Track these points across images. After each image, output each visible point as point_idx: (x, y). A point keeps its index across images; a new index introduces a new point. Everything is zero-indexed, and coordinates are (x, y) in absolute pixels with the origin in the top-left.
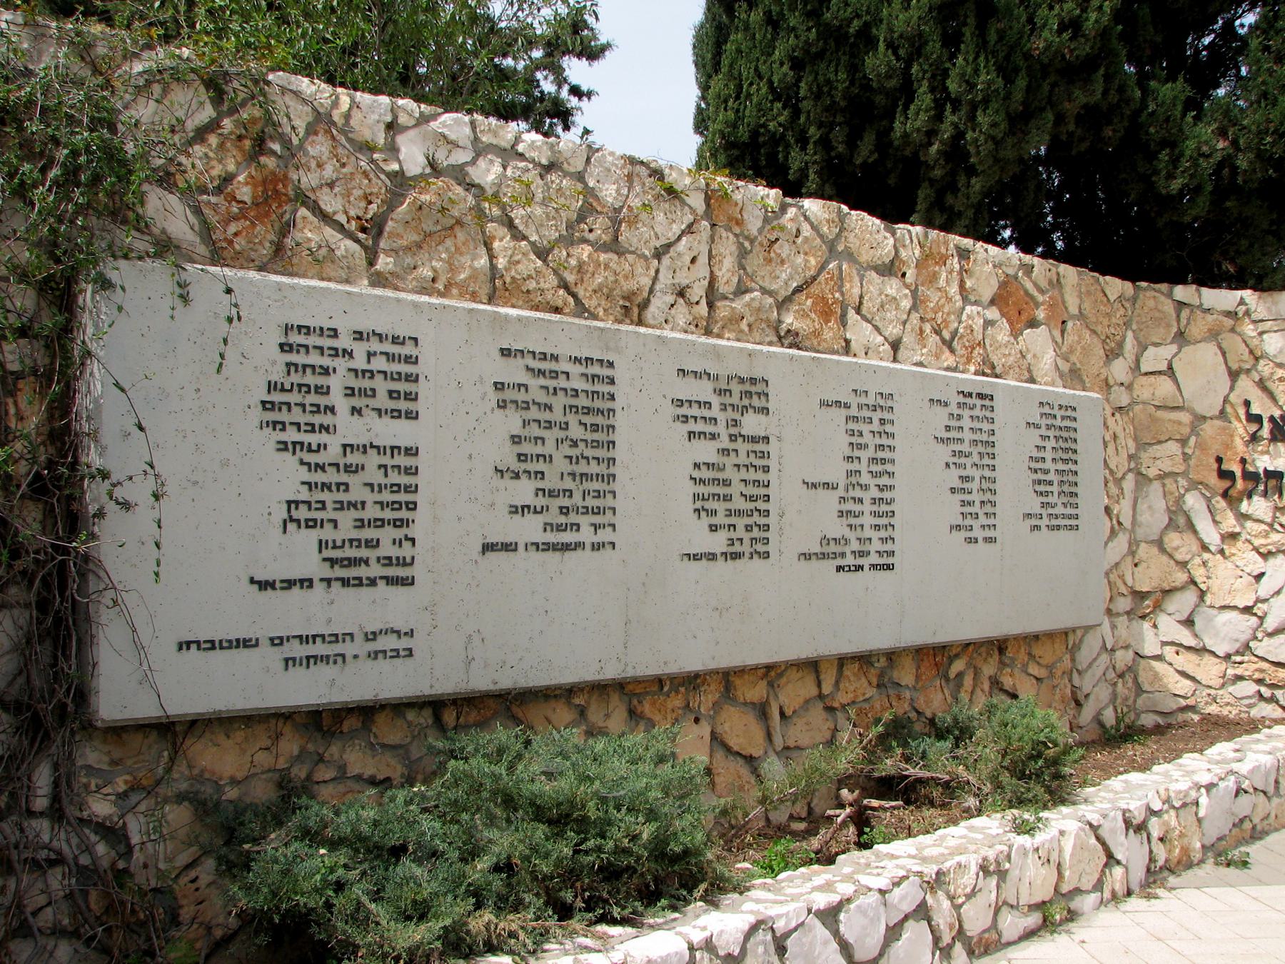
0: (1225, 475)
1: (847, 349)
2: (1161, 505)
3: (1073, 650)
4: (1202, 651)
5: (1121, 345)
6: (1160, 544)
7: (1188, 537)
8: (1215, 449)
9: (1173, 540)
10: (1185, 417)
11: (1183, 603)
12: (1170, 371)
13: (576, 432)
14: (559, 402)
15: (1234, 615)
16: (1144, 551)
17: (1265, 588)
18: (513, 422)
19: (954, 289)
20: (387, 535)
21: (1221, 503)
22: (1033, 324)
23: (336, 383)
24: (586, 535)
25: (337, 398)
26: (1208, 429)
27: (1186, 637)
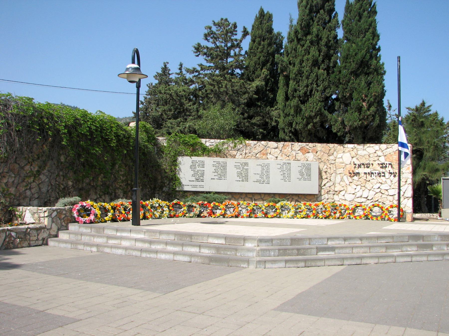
2: (340, 178)
3: (317, 198)
5: (333, 154)
6: (339, 184)
8: (349, 169)
9: (341, 183)
10: (344, 164)
12: (342, 158)
13: (222, 168)
14: (220, 166)
16: (337, 185)
17: (356, 191)
18: (215, 168)
19: (290, 149)
21: (349, 177)
22: (309, 152)
23: (197, 165)
25: (197, 166)
26: (347, 166)
27: (343, 198)
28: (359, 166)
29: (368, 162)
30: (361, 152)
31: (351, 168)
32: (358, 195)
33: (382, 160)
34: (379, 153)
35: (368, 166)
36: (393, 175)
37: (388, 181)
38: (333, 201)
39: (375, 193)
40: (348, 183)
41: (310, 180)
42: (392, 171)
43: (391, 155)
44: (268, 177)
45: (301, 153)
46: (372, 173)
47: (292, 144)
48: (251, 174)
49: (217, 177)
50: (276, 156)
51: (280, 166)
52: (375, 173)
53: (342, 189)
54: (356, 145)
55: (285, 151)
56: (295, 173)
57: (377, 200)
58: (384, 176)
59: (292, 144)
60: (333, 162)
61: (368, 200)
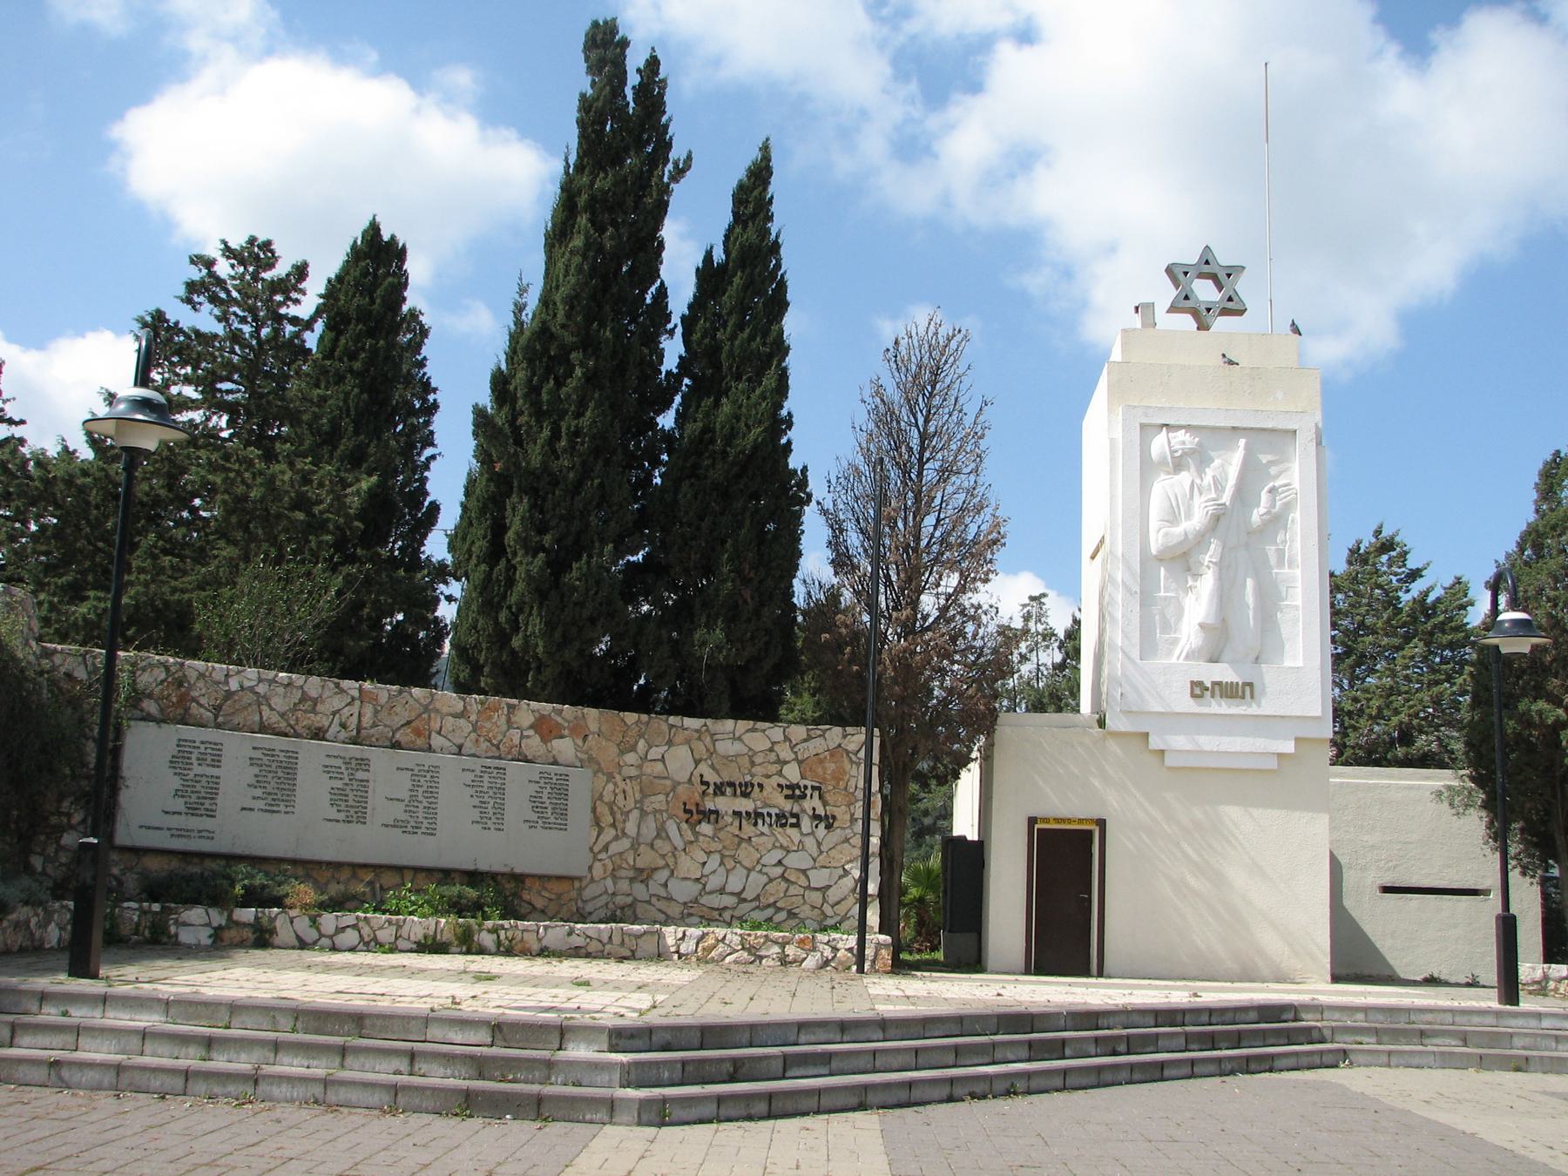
0: (686, 811)
1: (430, 749)
4: (670, 899)
6: (652, 846)
7: (667, 843)
8: (684, 798)
9: (658, 843)
10: (668, 783)
11: (662, 876)
12: (663, 759)
13: (280, 774)
15: (689, 883)
18: (256, 770)
20: (207, 802)
21: (684, 826)
23: (194, 756)
24: (282, 808)
25: (194, 760)
26: (680, 789)
27: (663, 893)
28: (719, 790)
29: (748, 778)
30: (726, 747)
31: (693, 794)
32: (714, 882)
33: (792, 773)
34: (785, 753)
35: (745, 791)
36: (822, 826)
37: (810, 843)
38: (629, 900)
39: (765, 879)
40: (679, 844)
41: (563, 828)
42: (820, 811)
43: (821, 762)
44: (431, 811)
45: (538, 738)
46: (758, 815)
47: (511, 707)
48: (376, 798)
49: (261, 804)
50: (459, 741)
51: (470, 776)
52: (769, 815)
53: (661, 863)
54: (709, 722)
55: (488, 725)
56: (517, 803)
57: (772, 900)
58: (797, 825)
59: (511, 707)
60: (633, 772)
61: (745, 900)
